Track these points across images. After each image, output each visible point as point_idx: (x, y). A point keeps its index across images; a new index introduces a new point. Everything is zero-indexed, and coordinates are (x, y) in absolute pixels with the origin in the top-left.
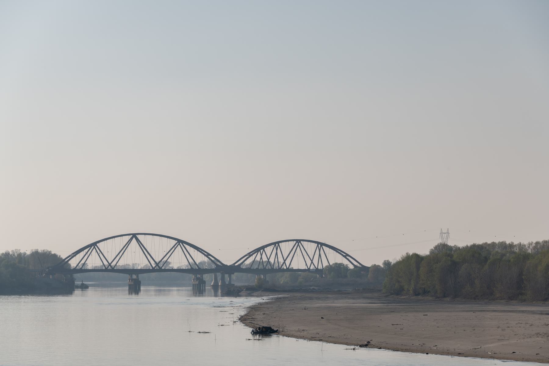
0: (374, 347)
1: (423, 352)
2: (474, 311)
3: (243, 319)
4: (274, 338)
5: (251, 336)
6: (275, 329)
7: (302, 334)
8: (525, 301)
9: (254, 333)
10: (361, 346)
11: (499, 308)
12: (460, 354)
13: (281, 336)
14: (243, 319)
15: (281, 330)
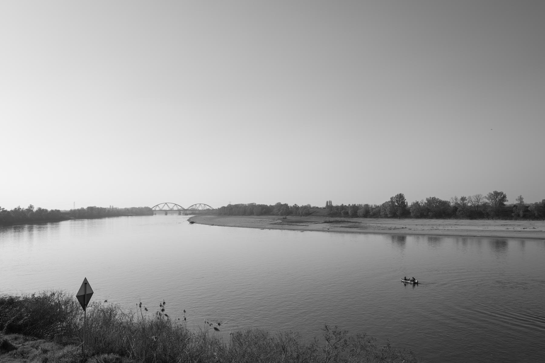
0: (214, 225)
3: (188, 220)
5: (189, 224)
10: (212, 225)
12: (231, 226)
14: (188, 220)
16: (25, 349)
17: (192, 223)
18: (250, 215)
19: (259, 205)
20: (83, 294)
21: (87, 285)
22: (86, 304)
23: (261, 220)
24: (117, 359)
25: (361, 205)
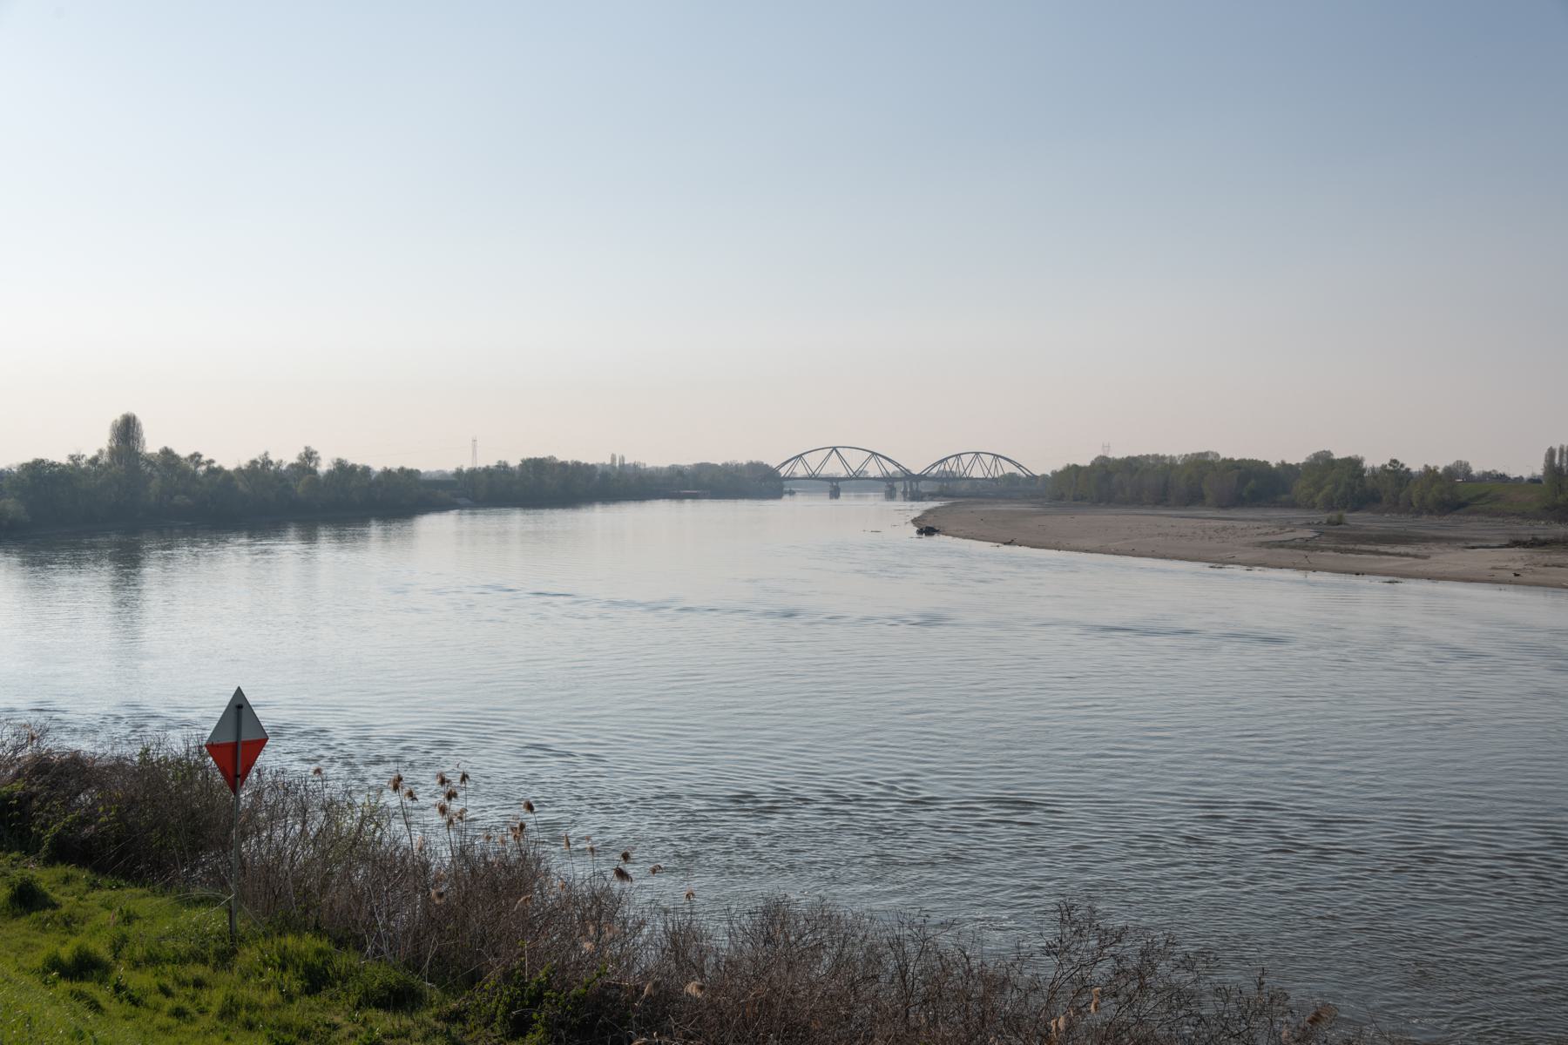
0: (1015, 544)
1: (1055, 549)
2: (1117, 515)
3: (915, 521)
4: (937, 538)
5: (915, 535)
6: (937, 529)
7: (957, 533)
8: (1167, 506)
9: (920, 532)
10: (1005, 544)
11: (1144, 511)
12: (1087, 551)
13: (941, 536)
14: (915, 521)
15: (941, 529)
16: (78, 910)
17: (928, 531)
18: (1187, 505)
19: (1231, 460)
20: (230, 739)
21: (243, 710)
22: (239, 773)
23: (1224, 529)
24: (319, 953)
25: (634, 465)
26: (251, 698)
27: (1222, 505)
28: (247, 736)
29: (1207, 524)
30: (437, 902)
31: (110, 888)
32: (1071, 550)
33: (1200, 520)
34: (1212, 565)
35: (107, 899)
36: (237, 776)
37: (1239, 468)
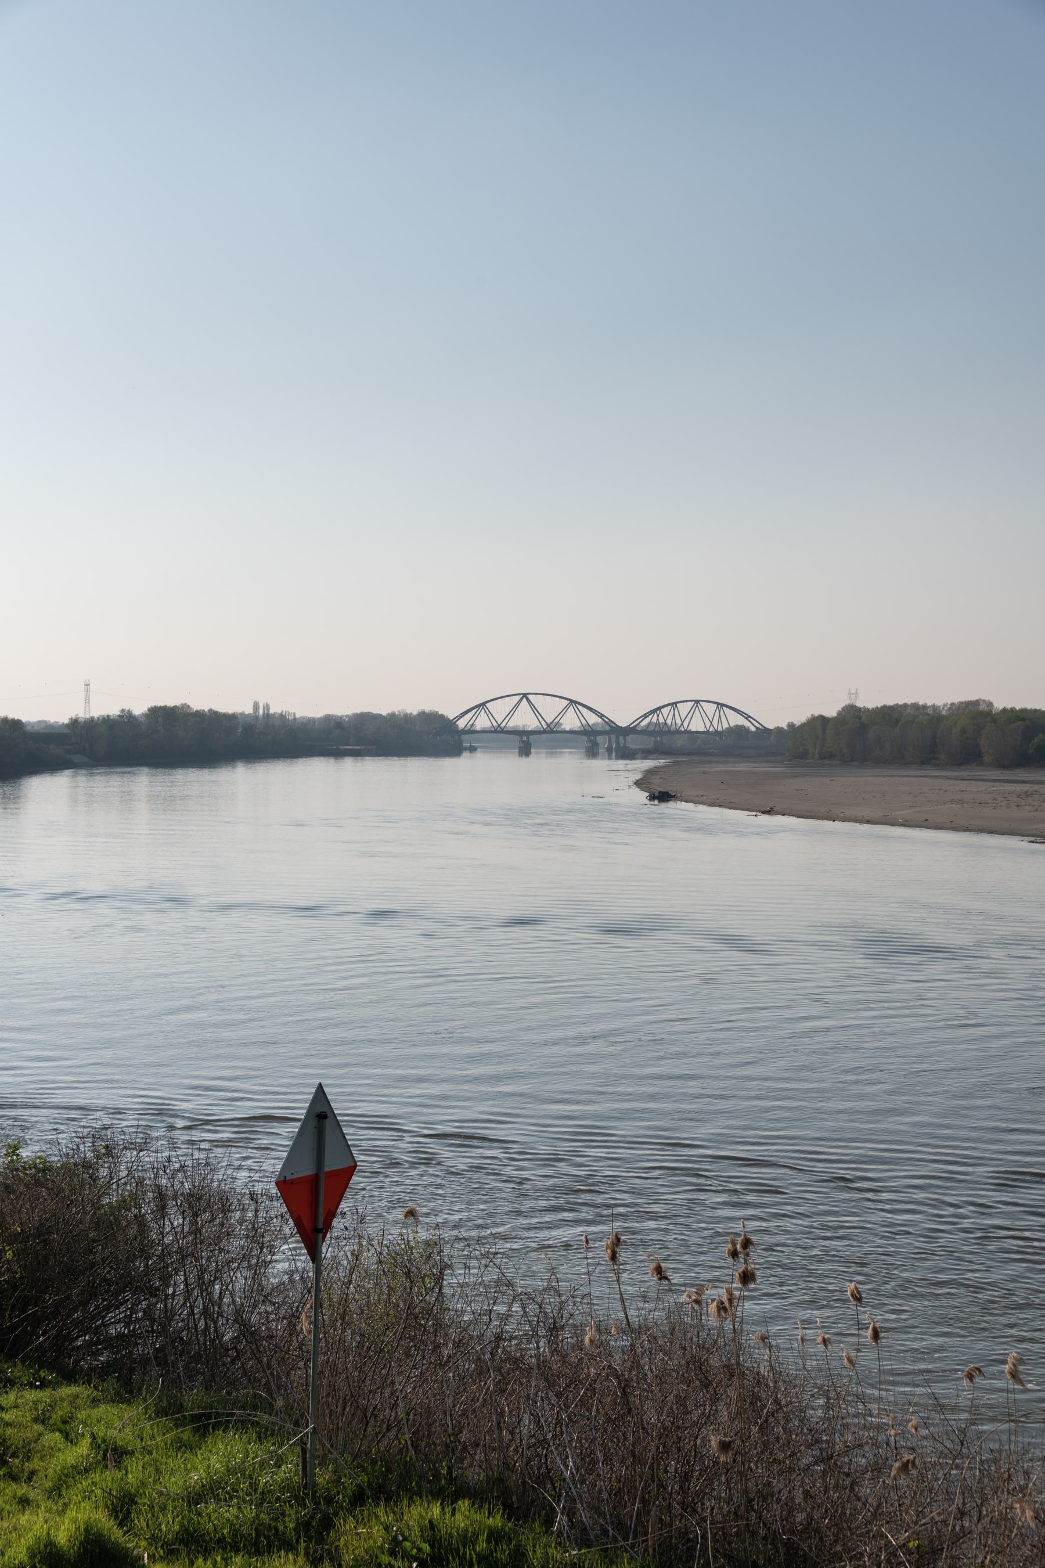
0: (777, 813)
1: (829, 819)
2: (884, 776)
3: (638, 784)
4: (671, 804)
5: (647, 802)
6: (673, 794)
7: (701, 799)
8: (938, 765)
9: (652, 798)
10: (763, 813)
13: (679, 802)
14: (638, 784)
15: (679, 795)
16: (9, 1431)
17: (664, 797)
18: (961, 764)
19: (1012, 710)
20: (306, 1170)
21: (328, 1123)
22: (320, 1225)
23: (1028, 794)
24: (495, 1536)
26: (338, 1108)
27: (1003, 764)
28: (331, 1164)
29: (1002, 788)
30: (722, 1458)
31: (32, 1385)
32: (850, 820)
33: (988, 784)
34: (1032, 839)
35: (40, 1407)
36: (318, 1231)
37: (1023, 719)
